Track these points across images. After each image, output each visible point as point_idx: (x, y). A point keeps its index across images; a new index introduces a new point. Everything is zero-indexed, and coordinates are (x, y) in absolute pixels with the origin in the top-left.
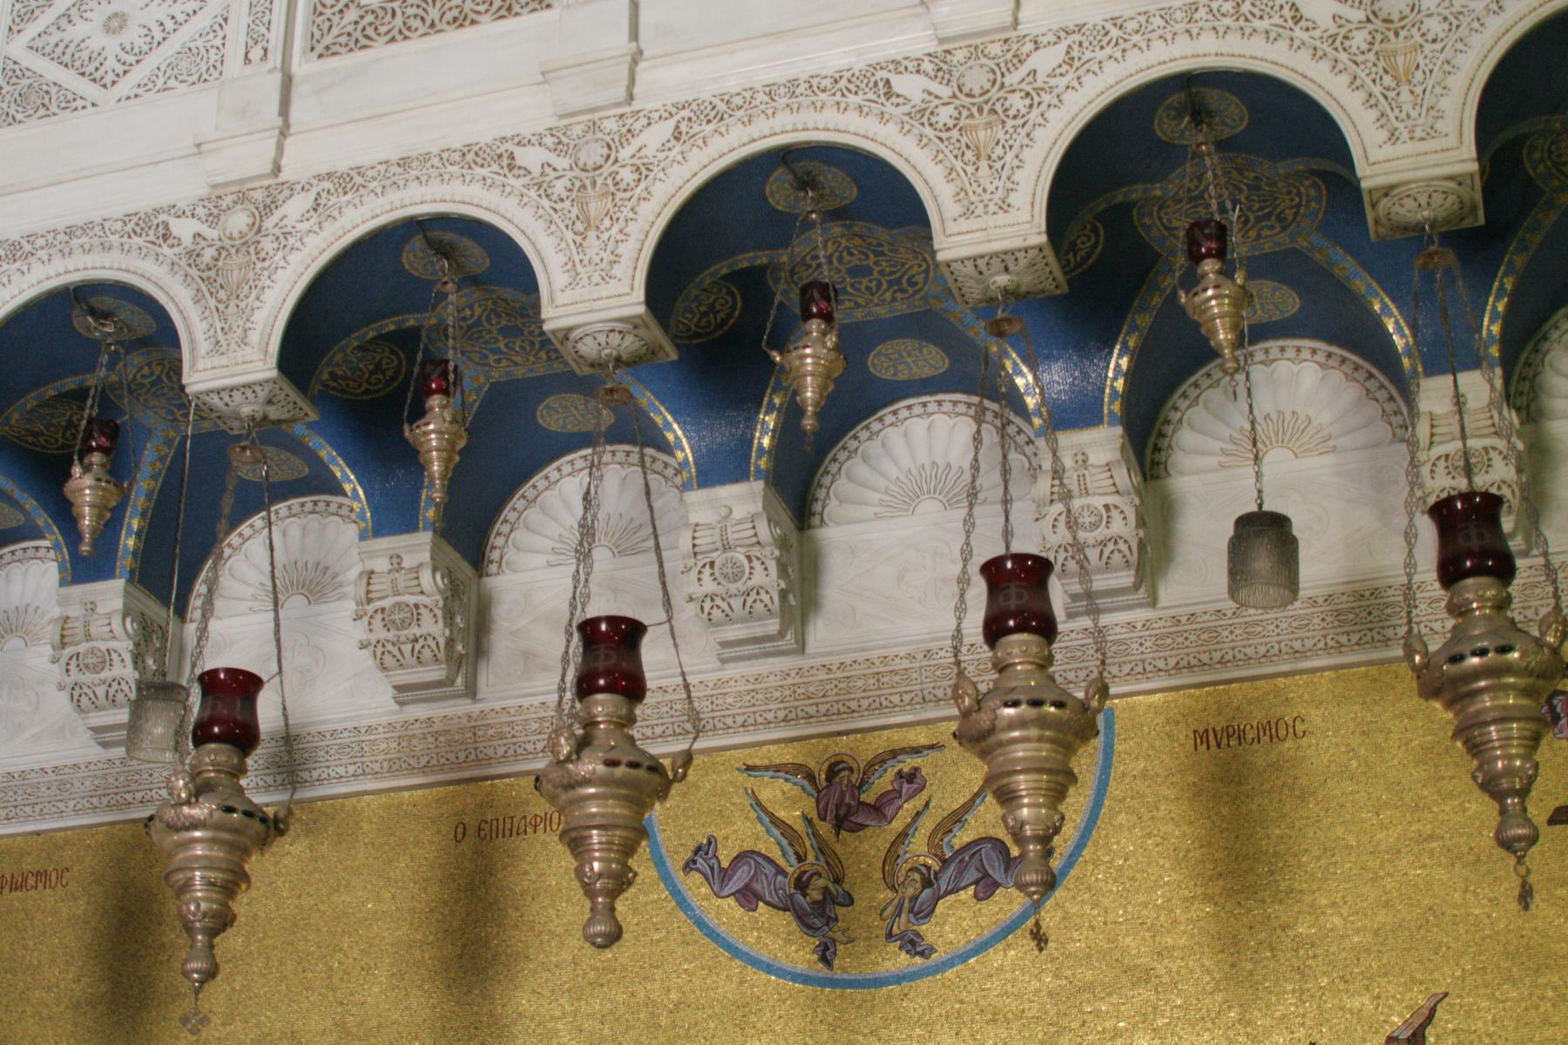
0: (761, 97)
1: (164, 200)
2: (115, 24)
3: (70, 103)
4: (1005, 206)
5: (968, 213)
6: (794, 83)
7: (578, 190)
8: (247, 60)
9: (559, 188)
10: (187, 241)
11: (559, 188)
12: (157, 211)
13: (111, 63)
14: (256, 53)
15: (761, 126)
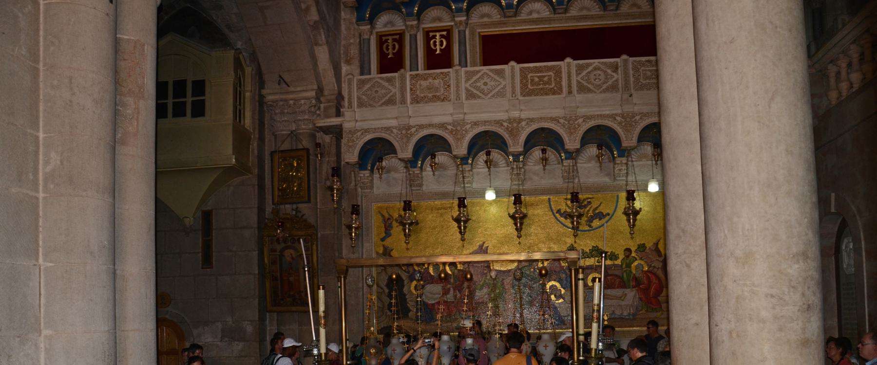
0: (596, 117)
1: (502, 119)
2: (485, 84)
3: (479, 97)
4: (632, 140)
5: (626, 140)
6: (601, 115)
7: (569, 128)
8: (512, 96)
9: (566, 126)
10: (506, 126)
11: (566, 126)
12: (500, 120)
13: (486, 91)
14: (514, 95)
15: (597, 121)
